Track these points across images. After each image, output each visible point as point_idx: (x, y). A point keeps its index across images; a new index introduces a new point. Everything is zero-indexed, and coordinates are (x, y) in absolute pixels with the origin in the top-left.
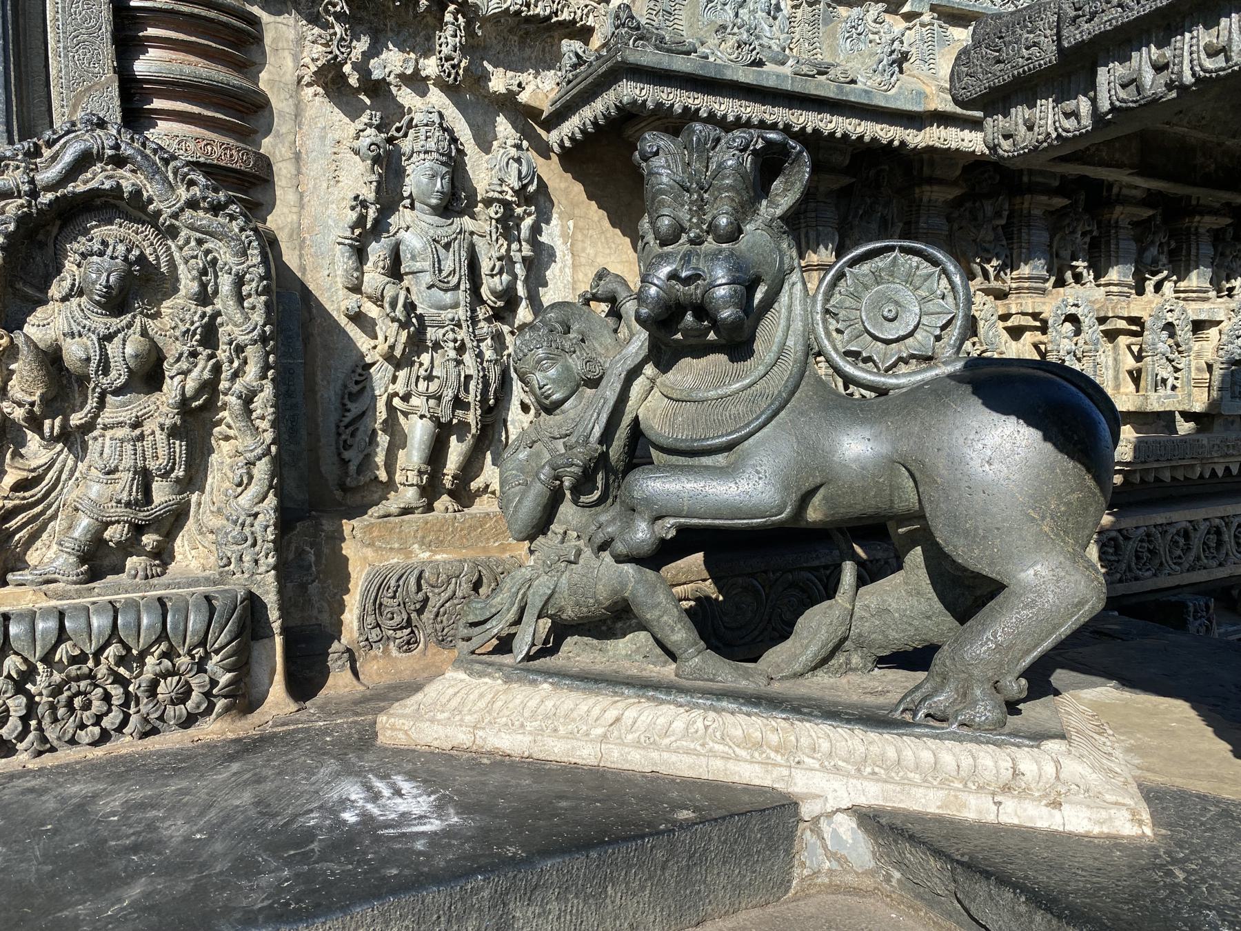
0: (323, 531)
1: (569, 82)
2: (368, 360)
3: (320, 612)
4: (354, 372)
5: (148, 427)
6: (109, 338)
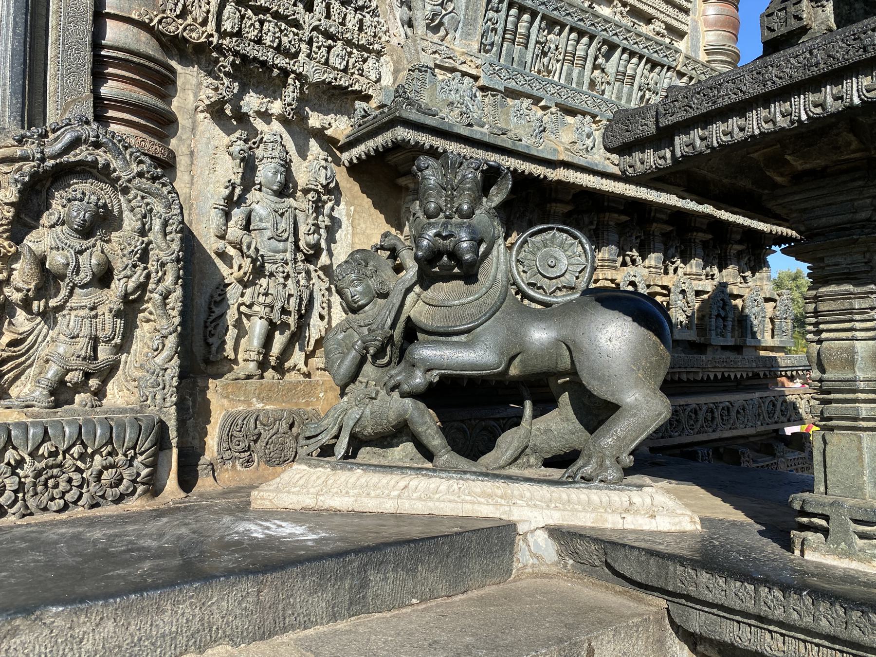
1: (360, 125)
2: (226, 281)
3: (193, 438)
5: (100, 310)
6: (81, 252)
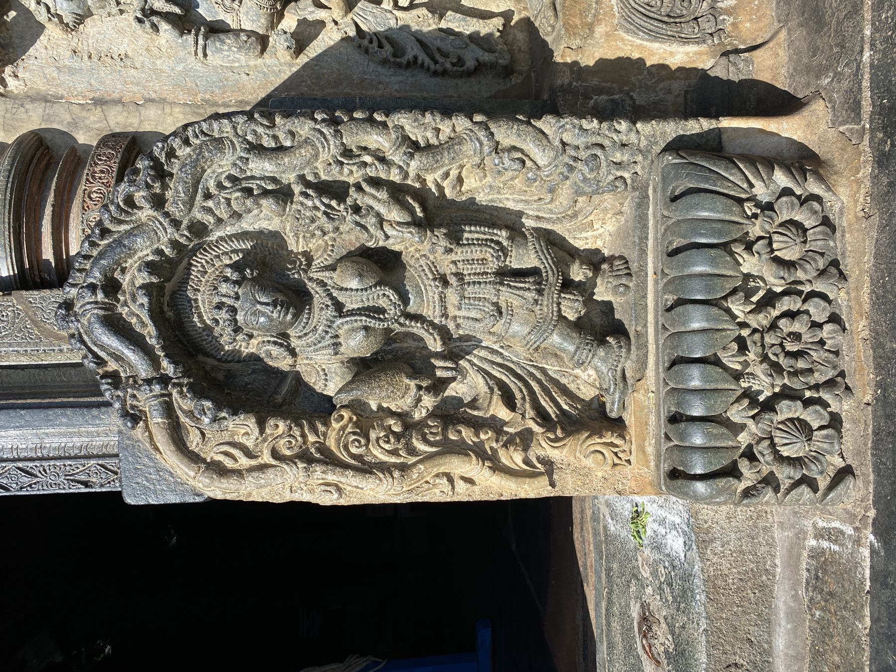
0: (570, 84)
2: (352, 33)
3: (669, 91)
4: (367, 51)
5: (447, 269)
6: (339, 307)
